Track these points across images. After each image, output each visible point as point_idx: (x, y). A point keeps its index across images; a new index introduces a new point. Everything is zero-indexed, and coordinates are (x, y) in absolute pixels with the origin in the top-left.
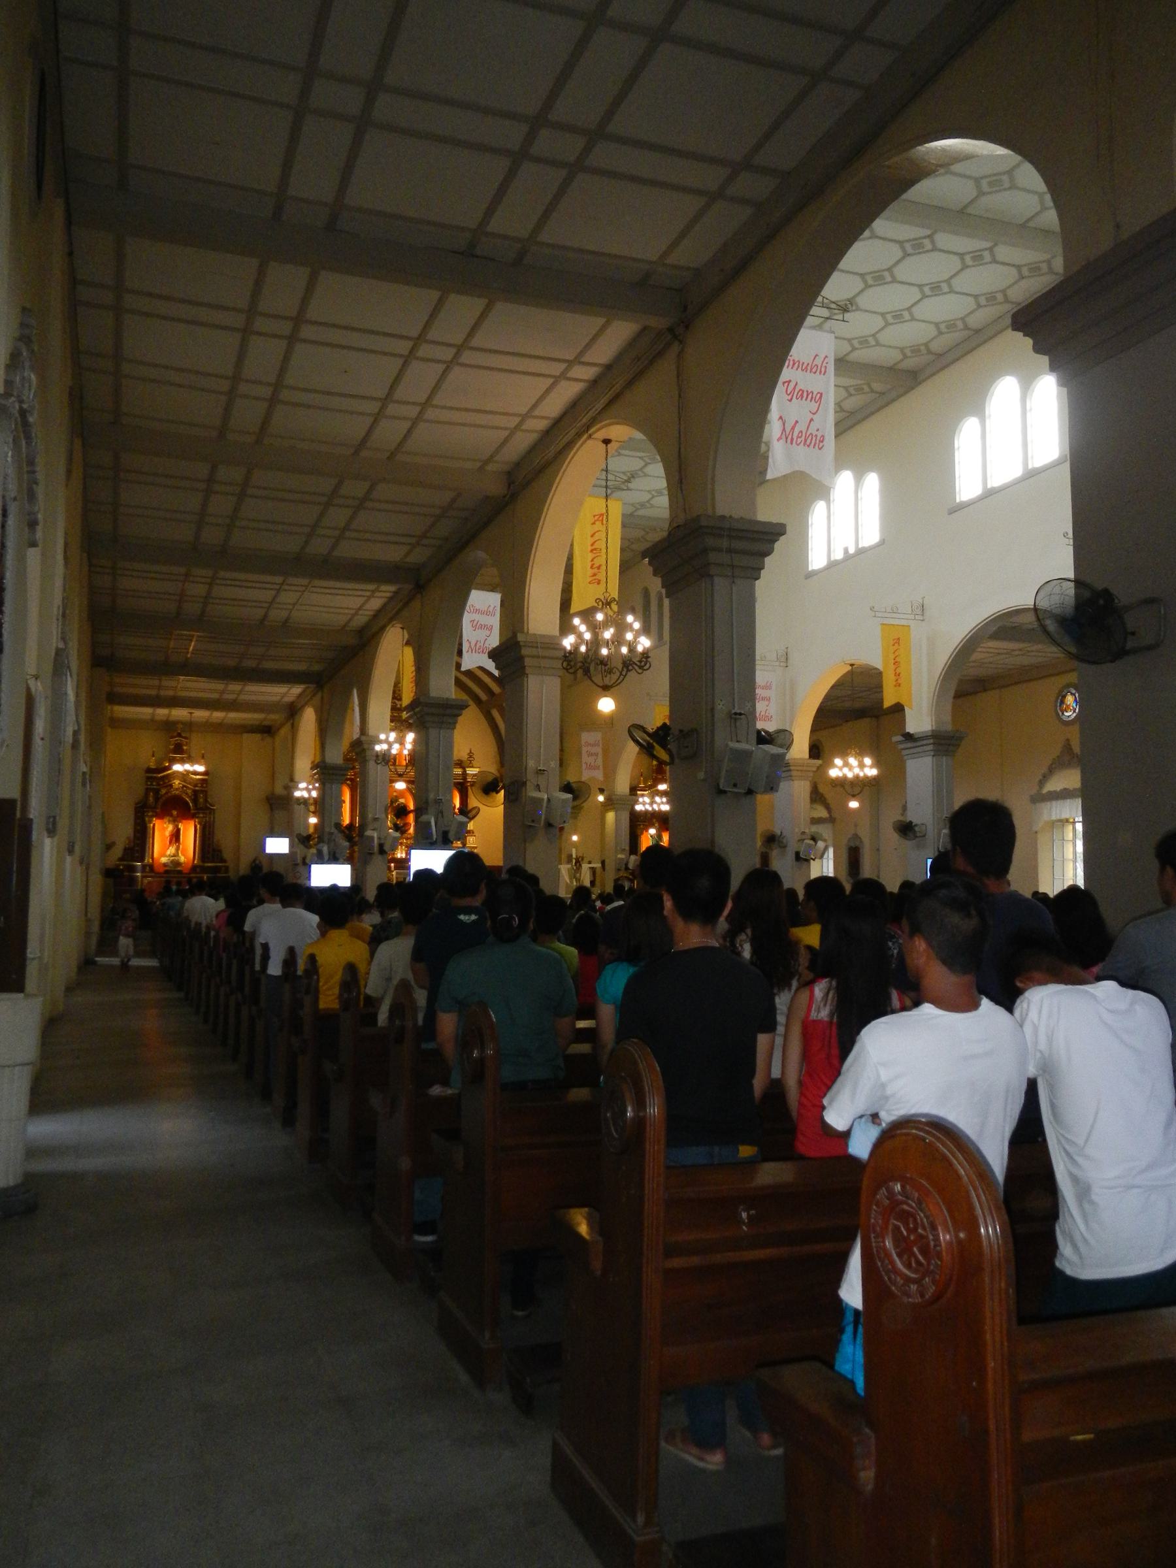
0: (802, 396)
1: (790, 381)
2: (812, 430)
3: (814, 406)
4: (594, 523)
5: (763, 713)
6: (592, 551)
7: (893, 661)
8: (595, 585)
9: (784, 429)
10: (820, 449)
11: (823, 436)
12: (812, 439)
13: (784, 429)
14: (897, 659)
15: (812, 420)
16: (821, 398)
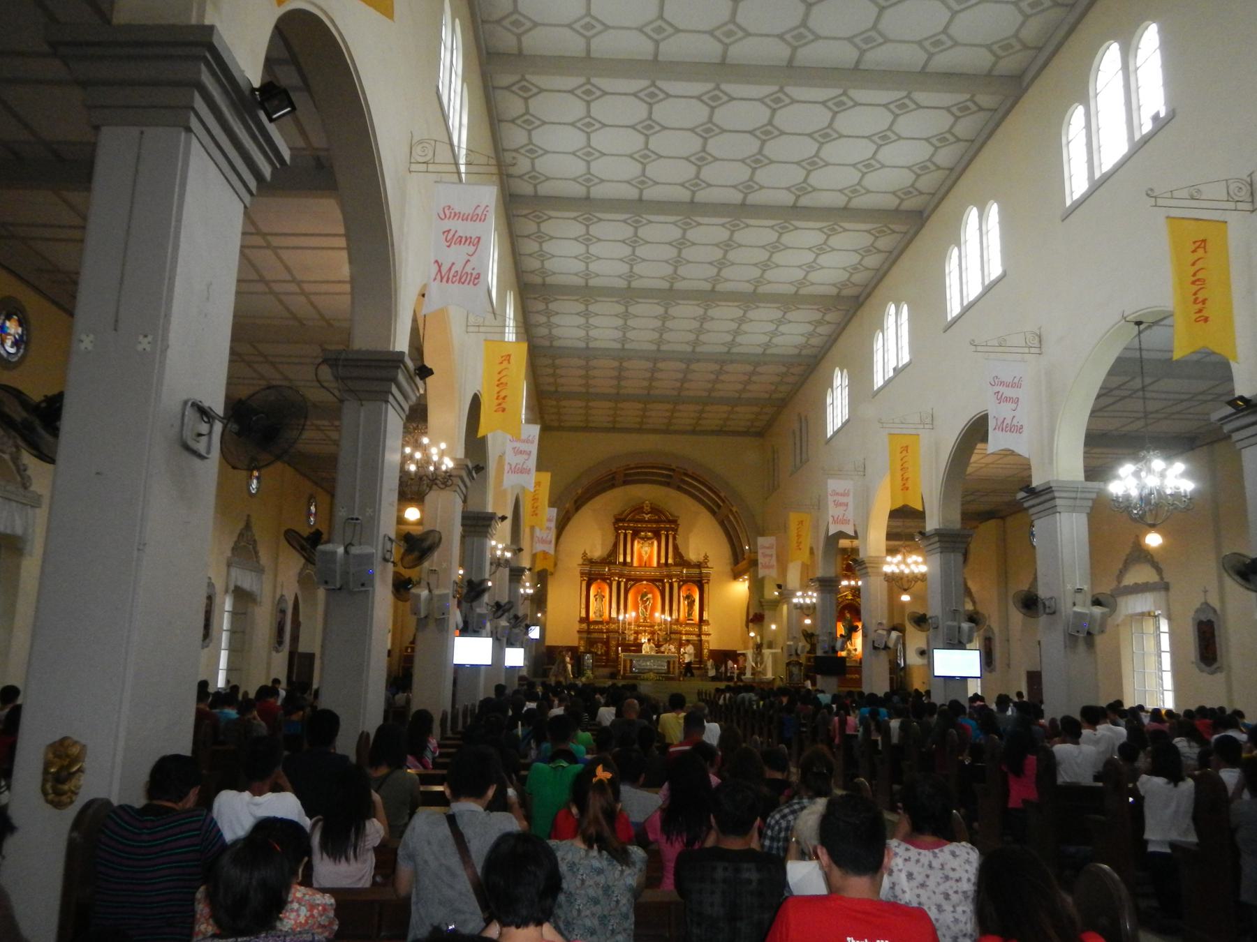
0: (461, 241)
1: (449, 231)
2: (468, 269)
3: (472, 249)
4: (501, 363)
5: (841, 517)
6: (498, 386)
7: (899, 467)
8: (501, 413)
9: (440, 271)
10: (475, 285)
11: (479, 274)
12: (465, 280)
13: (440, 271)
14: (905, 465)
15: (468, 261)
16: (478, 241)
